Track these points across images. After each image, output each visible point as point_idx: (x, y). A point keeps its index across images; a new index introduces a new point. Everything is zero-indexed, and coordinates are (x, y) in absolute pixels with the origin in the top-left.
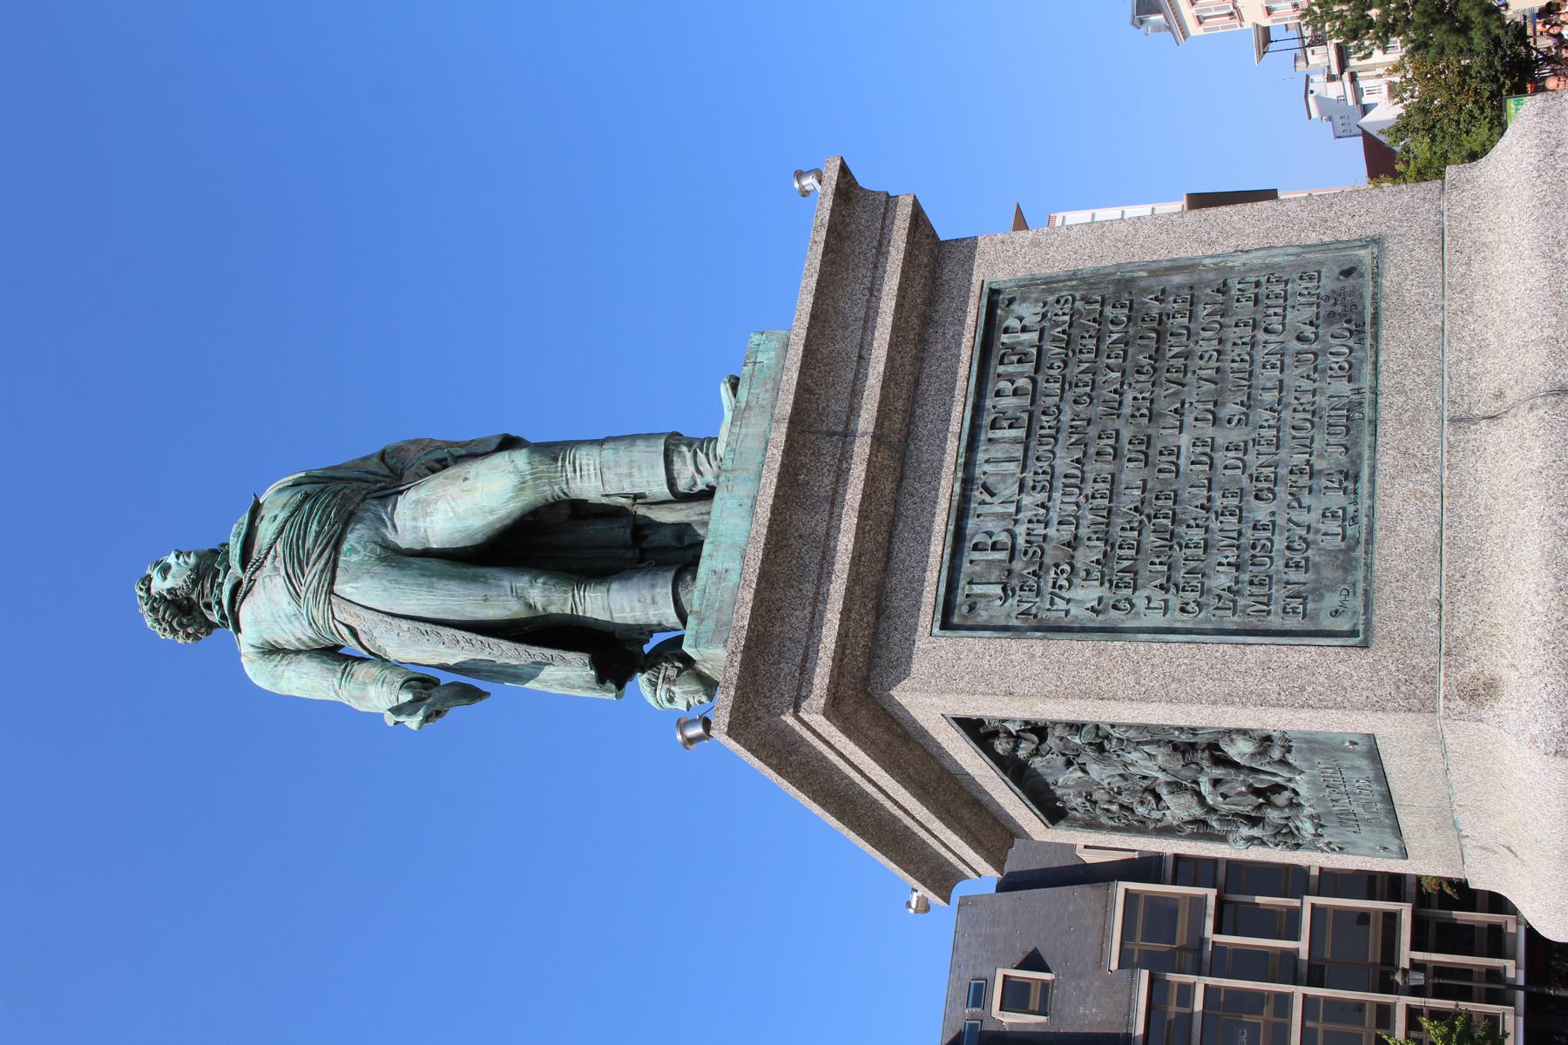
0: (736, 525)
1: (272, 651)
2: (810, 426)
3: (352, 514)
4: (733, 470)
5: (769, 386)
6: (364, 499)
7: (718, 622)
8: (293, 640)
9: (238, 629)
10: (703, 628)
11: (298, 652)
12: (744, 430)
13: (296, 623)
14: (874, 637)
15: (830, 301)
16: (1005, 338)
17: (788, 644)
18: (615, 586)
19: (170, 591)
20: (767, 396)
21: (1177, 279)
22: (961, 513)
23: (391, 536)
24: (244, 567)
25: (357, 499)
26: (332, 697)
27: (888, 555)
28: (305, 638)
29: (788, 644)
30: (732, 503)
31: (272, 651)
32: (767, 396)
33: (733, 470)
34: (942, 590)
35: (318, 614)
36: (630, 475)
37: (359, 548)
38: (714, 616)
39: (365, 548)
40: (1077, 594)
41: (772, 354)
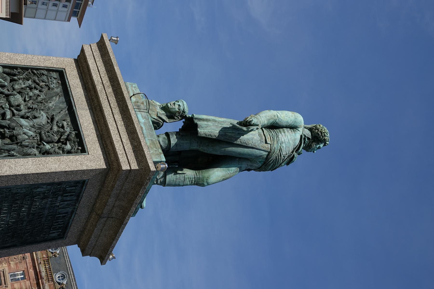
1: (293, 127)
8: (286, 133)
9: (301, 136)
11: (286, 127)
13: (283, 140)
14: (106, 177)
16: (60, 230)
18: (188, 149)
19: (319, 144)
21: (8, 245)
22: (78, 200)
24: (294, 155)
26: (280, 112)
27: (100, 192)
28: (283, 133)
31: (293, 127)
34: (84, 188)
35: (275, 146)
36: (176, 179)
40: (42, 190)
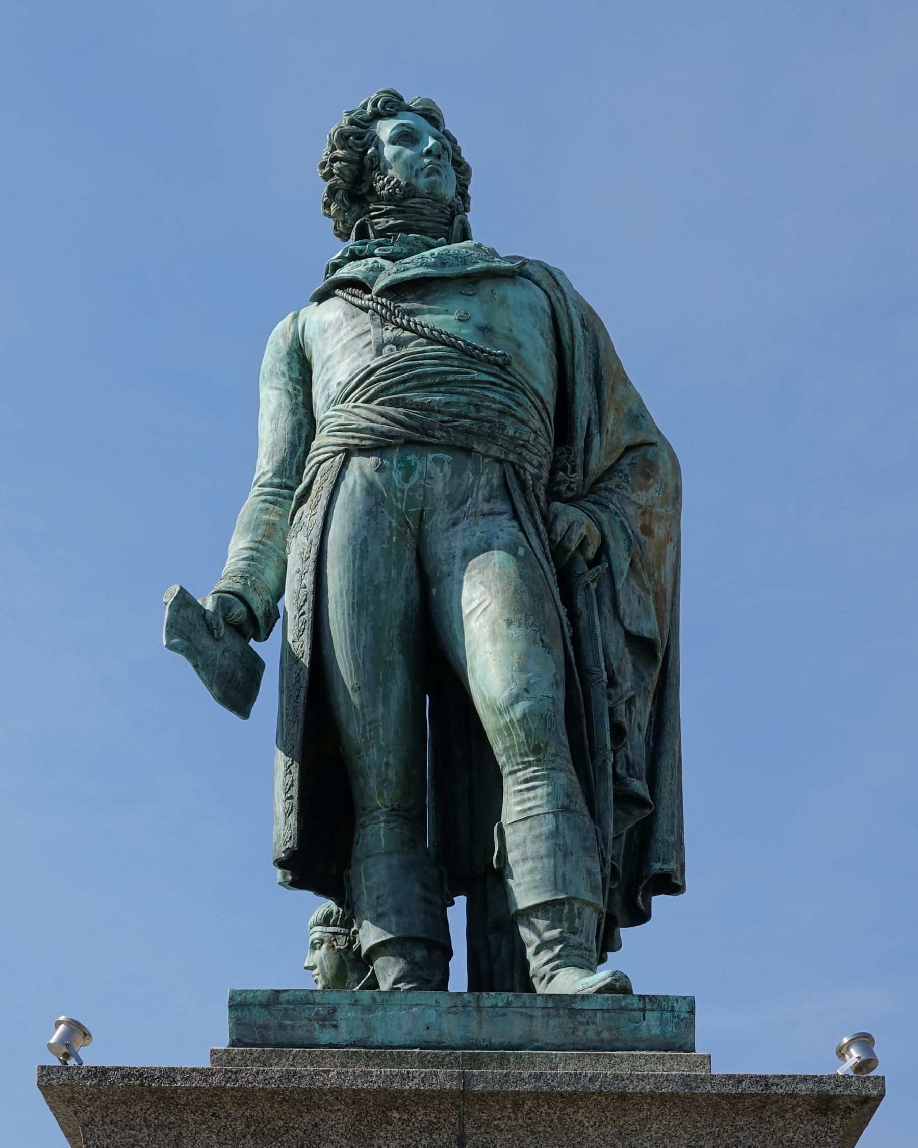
0: (400, 1027)
2: (469, 1115)
3: (468, 451)
4: (479, 1008)
5: (605, 1035)
6: (500, 461)
7: (266, 1027)
10: (255, 1011)
12: (538, 1013)
15: (655, 1111)
17: (174, 1132)
20: (591, 1035)
23: (441, 518)
25: (494, 451)
29: (174, 1132)
30: (431, 1016)
32: (591, 1035)
33: (479, 1008)
37: (414, 479)
38: (274, 1022)
39: (412, 489)
41: (656, 1031)
